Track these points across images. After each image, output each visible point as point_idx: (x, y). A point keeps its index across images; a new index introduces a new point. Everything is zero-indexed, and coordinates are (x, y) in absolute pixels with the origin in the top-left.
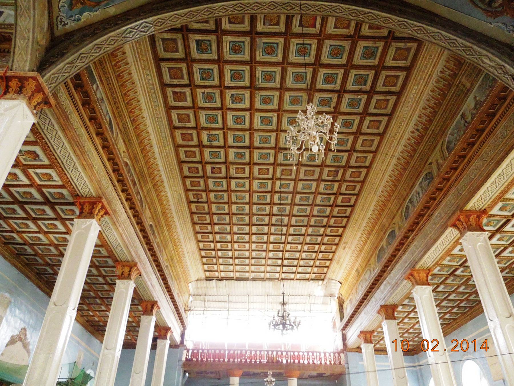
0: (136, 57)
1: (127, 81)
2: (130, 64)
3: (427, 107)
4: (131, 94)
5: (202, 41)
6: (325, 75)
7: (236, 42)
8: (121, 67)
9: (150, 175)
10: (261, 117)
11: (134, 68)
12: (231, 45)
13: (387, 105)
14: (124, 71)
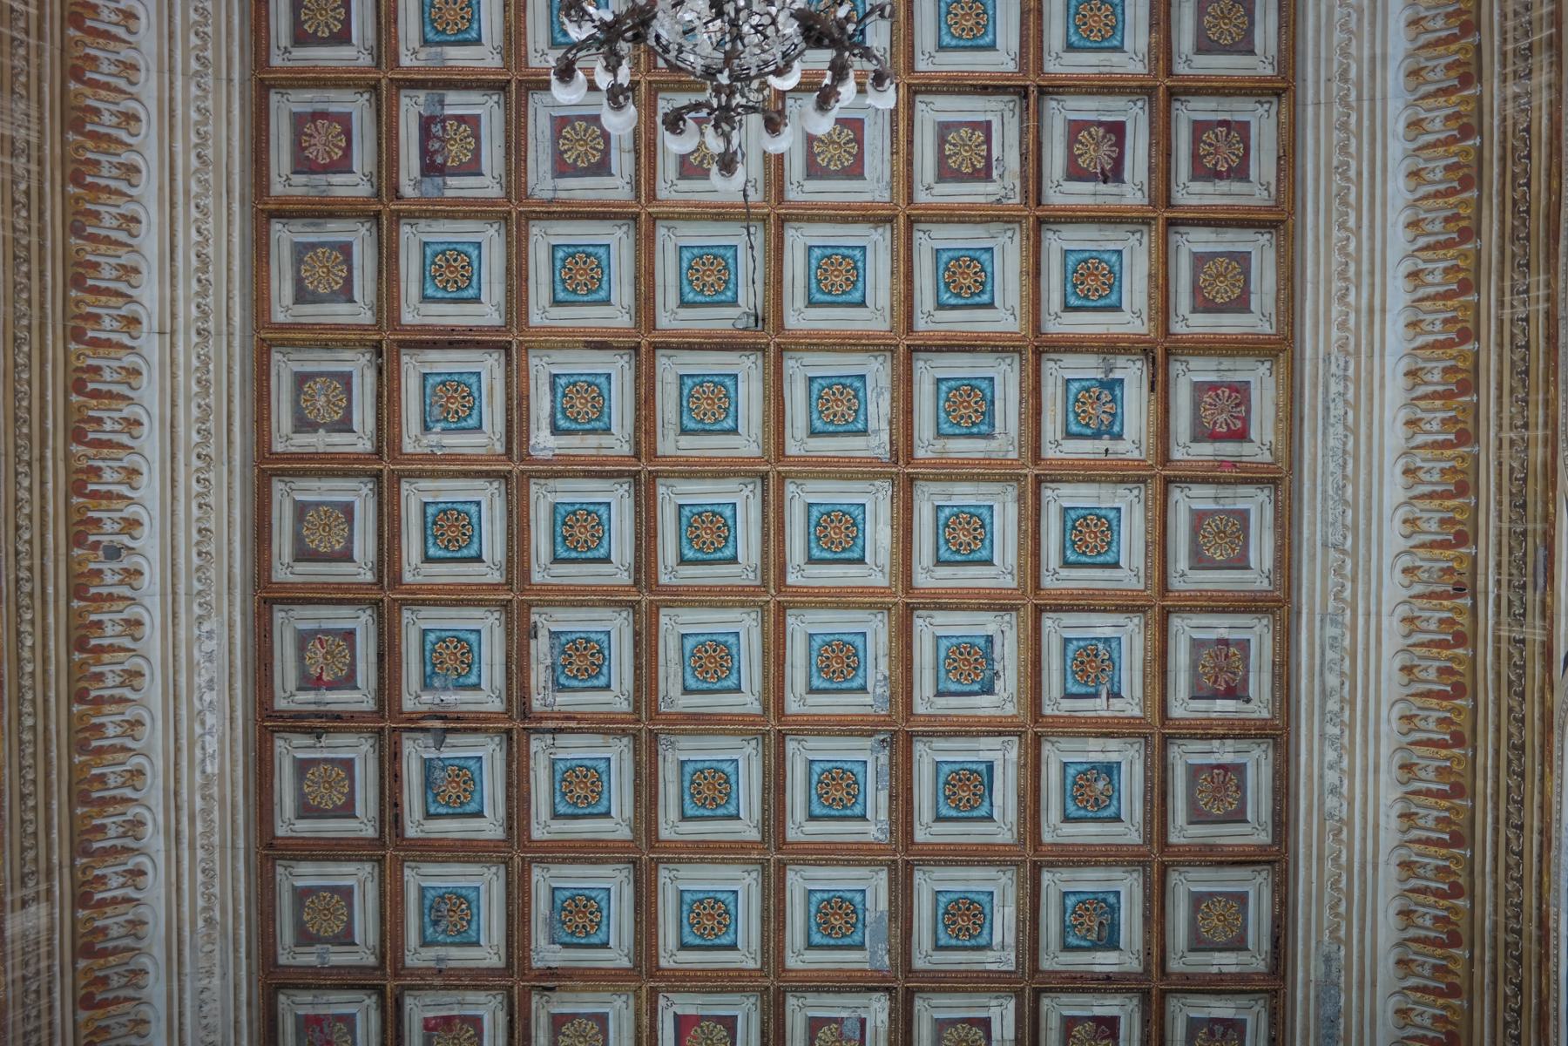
0: (1364, 882)
1: (1428, 793)
2: (1395, 860)
3: (127, 693)
4: (1432, 726)
5: (1094, 947)
6: (601, 809)
7: (965, 948)
8: (1437, 868)
9: (1469, 177)
10: (861, 561)
11: (1382, 834)
12: (986, 931)
13: (301, 659)
14: (1427, 842)
